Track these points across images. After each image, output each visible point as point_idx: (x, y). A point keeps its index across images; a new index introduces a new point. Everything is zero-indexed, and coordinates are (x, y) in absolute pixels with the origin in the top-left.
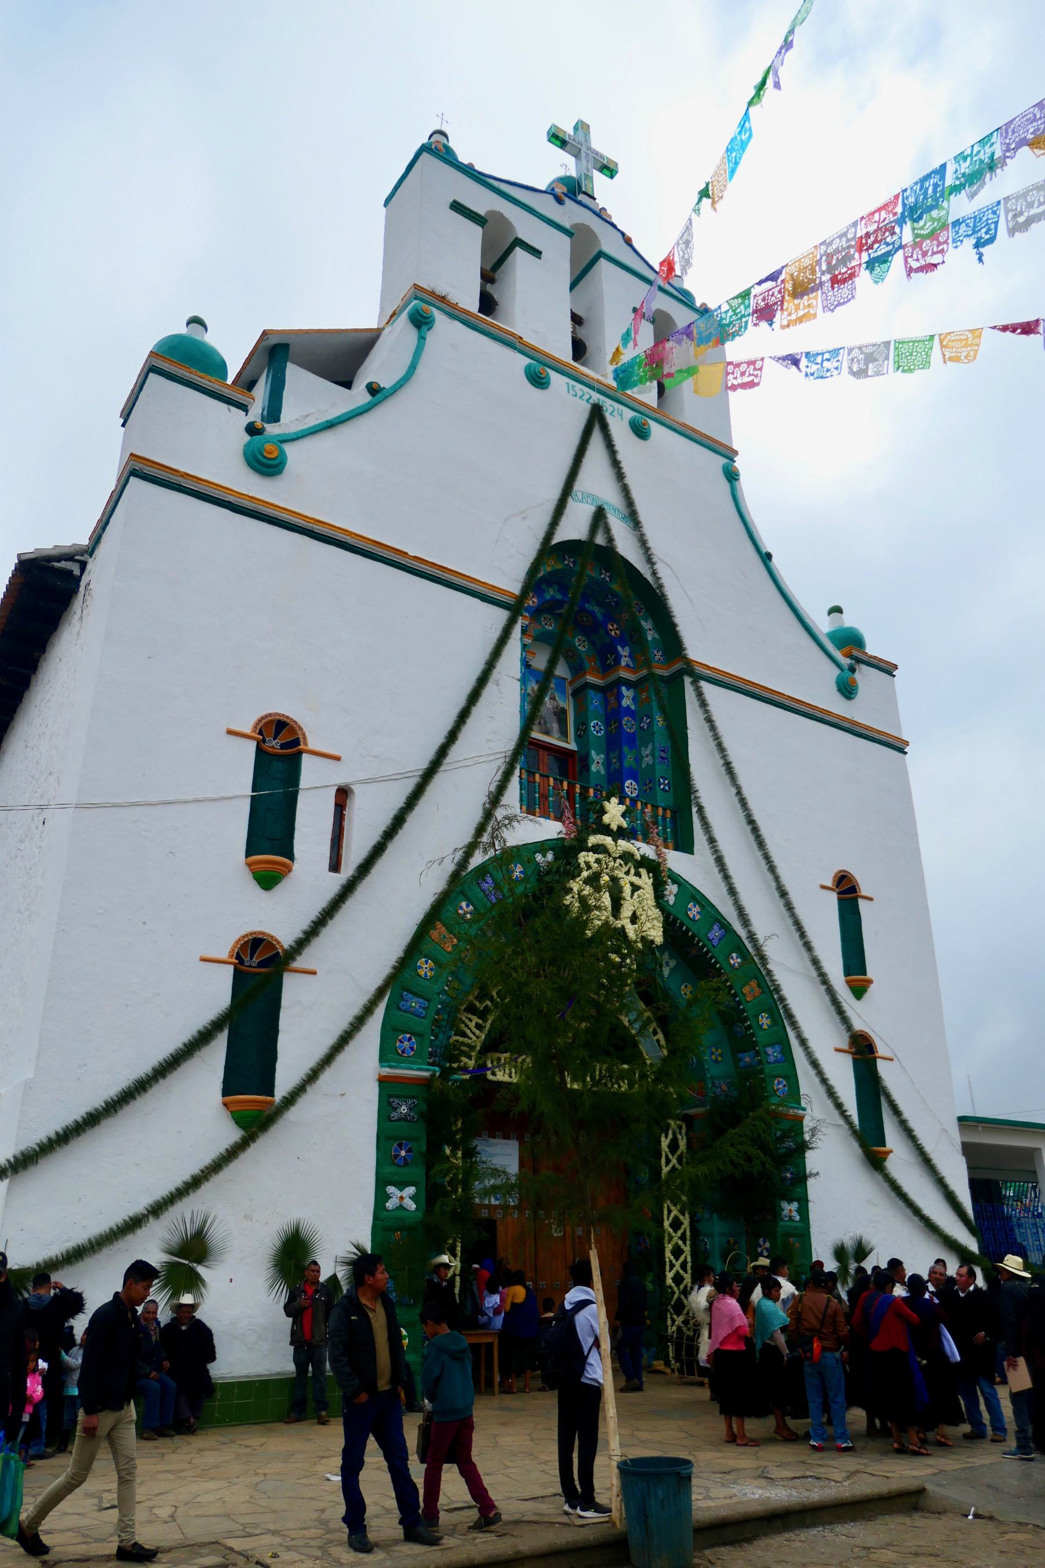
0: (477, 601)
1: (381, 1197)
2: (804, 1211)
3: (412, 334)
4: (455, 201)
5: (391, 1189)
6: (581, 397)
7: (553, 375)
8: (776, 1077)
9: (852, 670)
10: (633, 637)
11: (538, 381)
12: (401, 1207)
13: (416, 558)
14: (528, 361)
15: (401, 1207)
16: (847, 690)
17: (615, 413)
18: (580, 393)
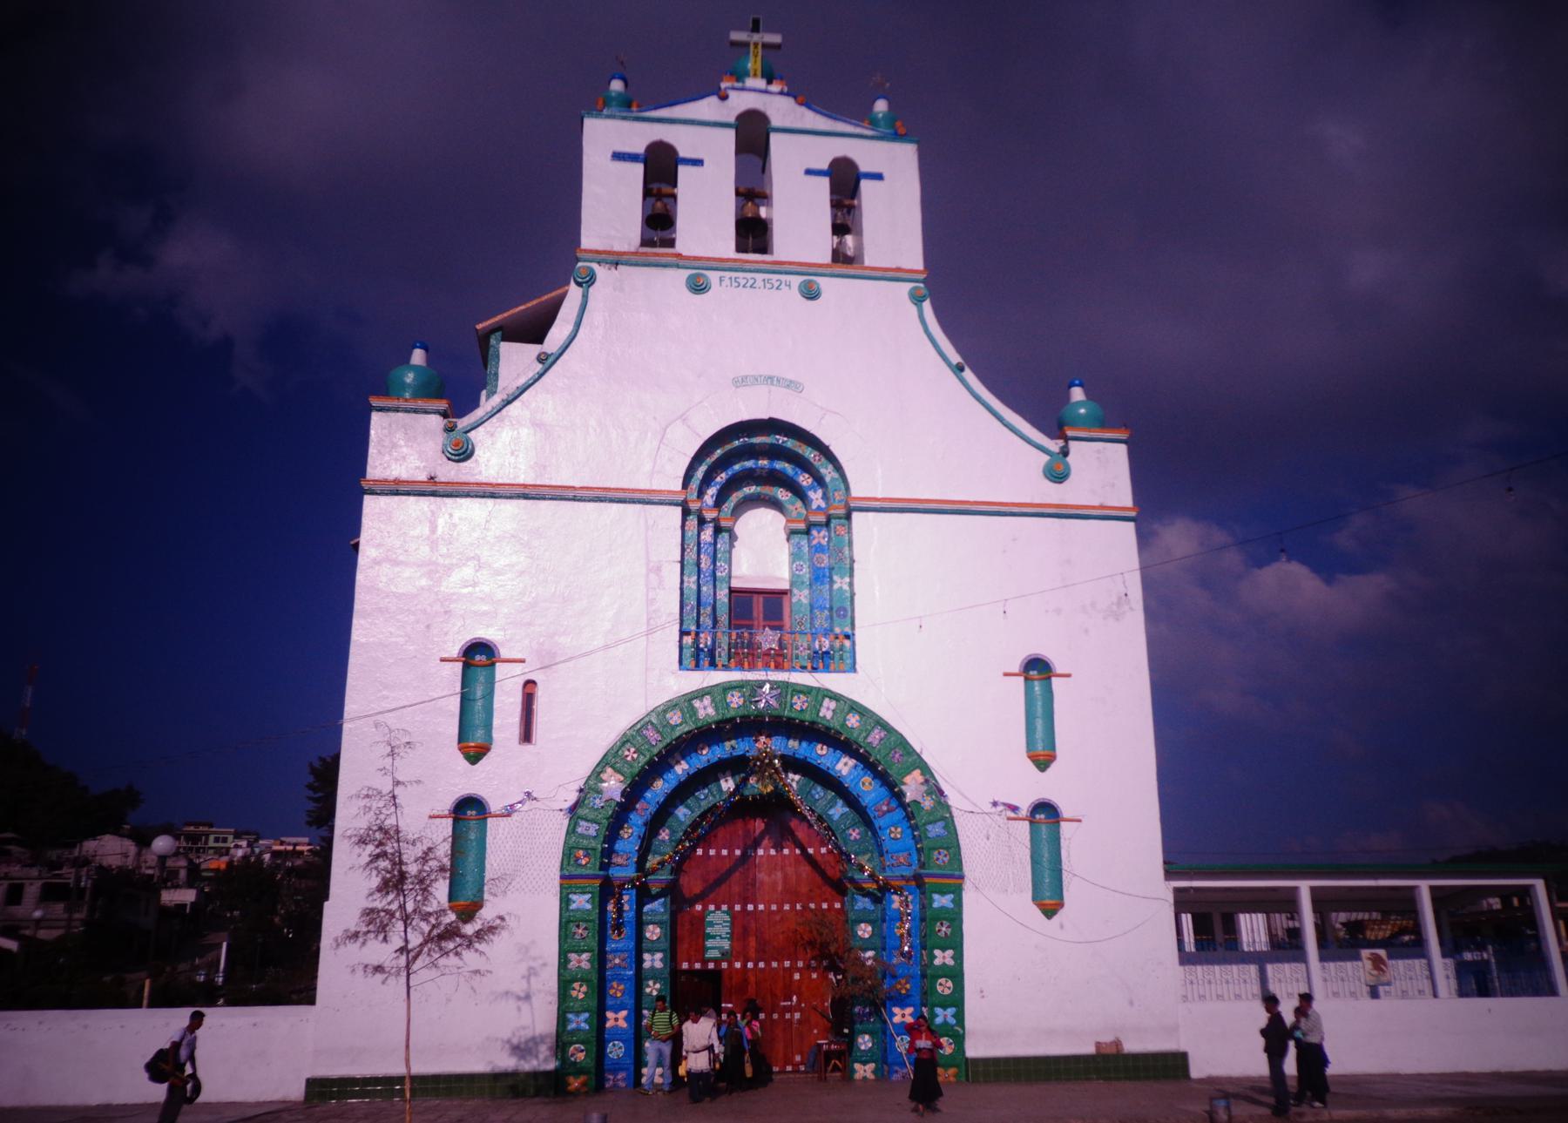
0: (638, 507)
2: (959, 957)
6: (744, 286)
7: (713, 276)
8: (935, 849)
9: (1065, 452)
11: (698, 287)
14: (685, 273)
16: (1057, 474)
17: (783, 286)
18: (743, 282)
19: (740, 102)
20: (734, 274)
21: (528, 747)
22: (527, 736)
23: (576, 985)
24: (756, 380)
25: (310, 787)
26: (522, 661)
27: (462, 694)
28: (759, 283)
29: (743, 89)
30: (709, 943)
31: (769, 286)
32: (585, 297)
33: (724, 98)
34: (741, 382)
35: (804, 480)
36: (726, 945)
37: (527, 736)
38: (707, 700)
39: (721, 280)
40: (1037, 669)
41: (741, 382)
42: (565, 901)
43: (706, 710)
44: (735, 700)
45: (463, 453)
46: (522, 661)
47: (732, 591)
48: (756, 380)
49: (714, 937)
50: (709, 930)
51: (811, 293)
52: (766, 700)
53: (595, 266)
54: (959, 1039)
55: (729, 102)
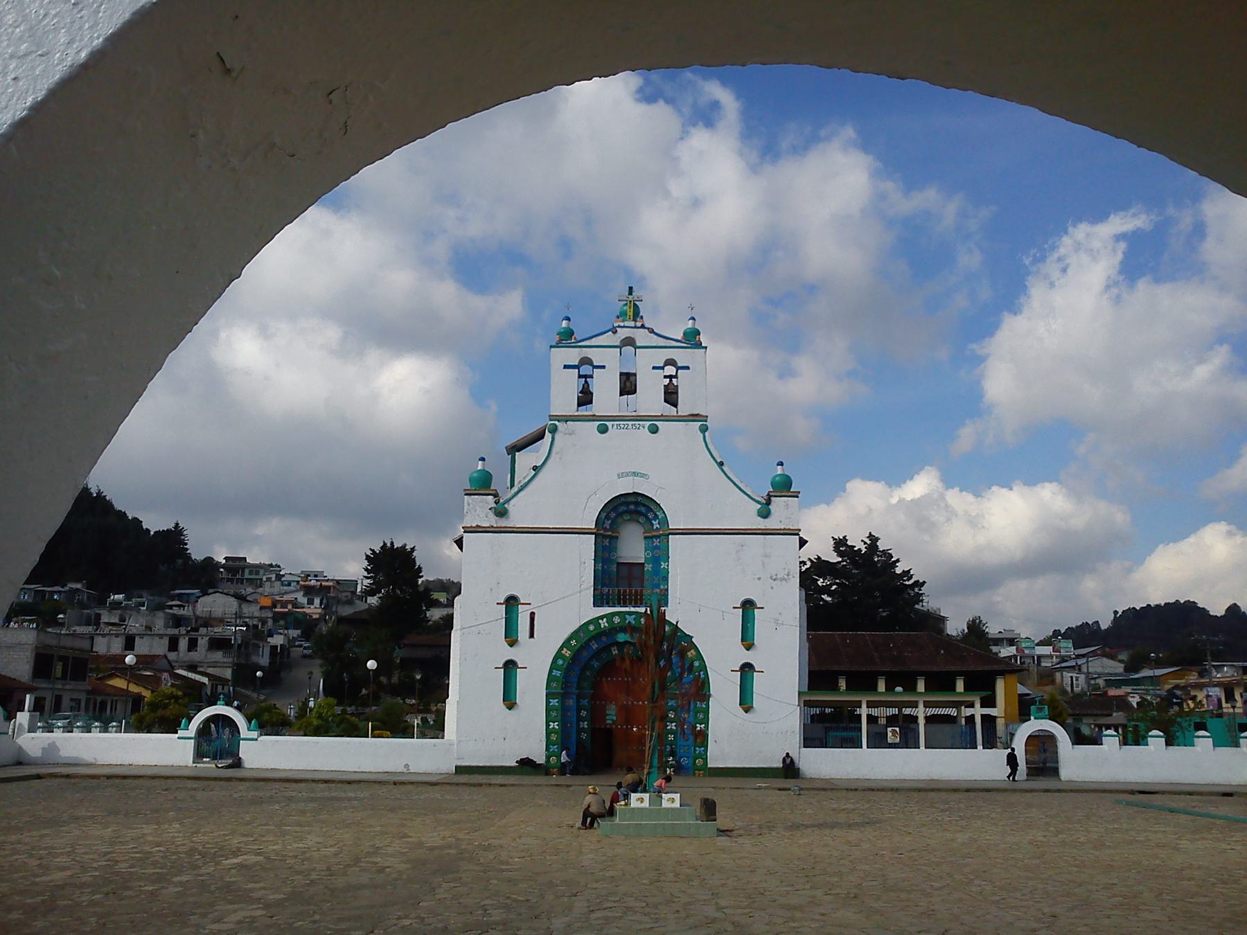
1: (548, 725)
3: (550, 435)
4: (565, 365)
5: (551, 723)
7: (609, 424)
9: (768, 502)
10: (656, 517)
11: (603, 430)
12: (554, 728)
13: (553, 528)
15: (554, 728)
16: (765, 514)
19: (623, 333)
20: (618, 423)
21: (532, 639)
22: (532, 635)
23: (553, 735)
24: (627, 474)
25: (366, 570)
26: (530, 604)
27: (506, 618)
28: (630, 427)
29: (624, 327)
30: (607, 718)
31: (634, 427)
32: (553, 439)
33: (615, 332)
34: (620, 476)
35: (650, 516)
36: (615, 718)
37: (532, 635)
38: (605, 620)
39: (613, 426)
40: (748, 605)
41: (620, 476)
42: (548, 703)
43: (604, 623)
44: (617, 620)
45: (501, 513)
46: (530, 604)
47: (619, 564)
48: (627, 474)
49: (610, 715)
50: (607, 712)
51: (654, 430)
52: (630, 619)
53: (556, 423)
54: (705, 760)
55: (618, 335)
